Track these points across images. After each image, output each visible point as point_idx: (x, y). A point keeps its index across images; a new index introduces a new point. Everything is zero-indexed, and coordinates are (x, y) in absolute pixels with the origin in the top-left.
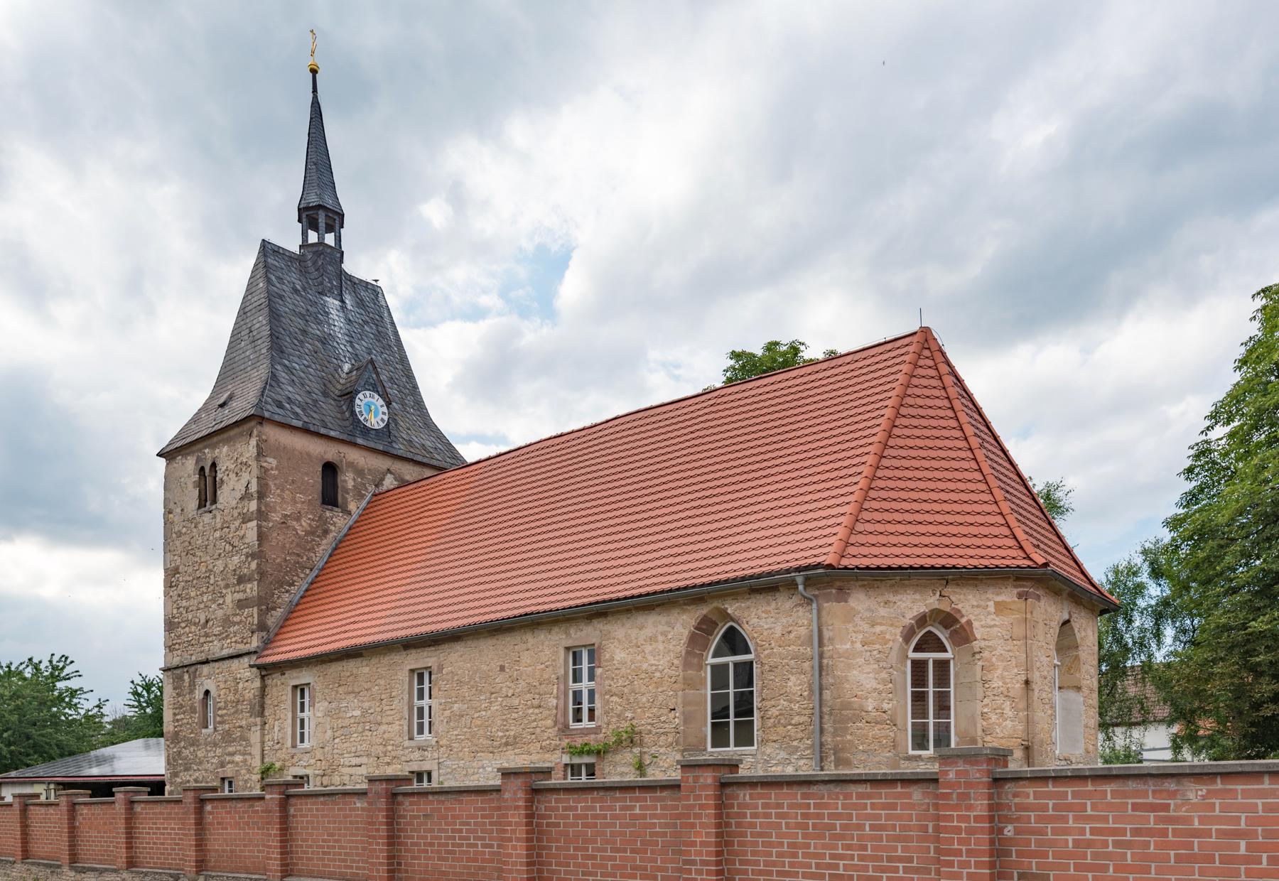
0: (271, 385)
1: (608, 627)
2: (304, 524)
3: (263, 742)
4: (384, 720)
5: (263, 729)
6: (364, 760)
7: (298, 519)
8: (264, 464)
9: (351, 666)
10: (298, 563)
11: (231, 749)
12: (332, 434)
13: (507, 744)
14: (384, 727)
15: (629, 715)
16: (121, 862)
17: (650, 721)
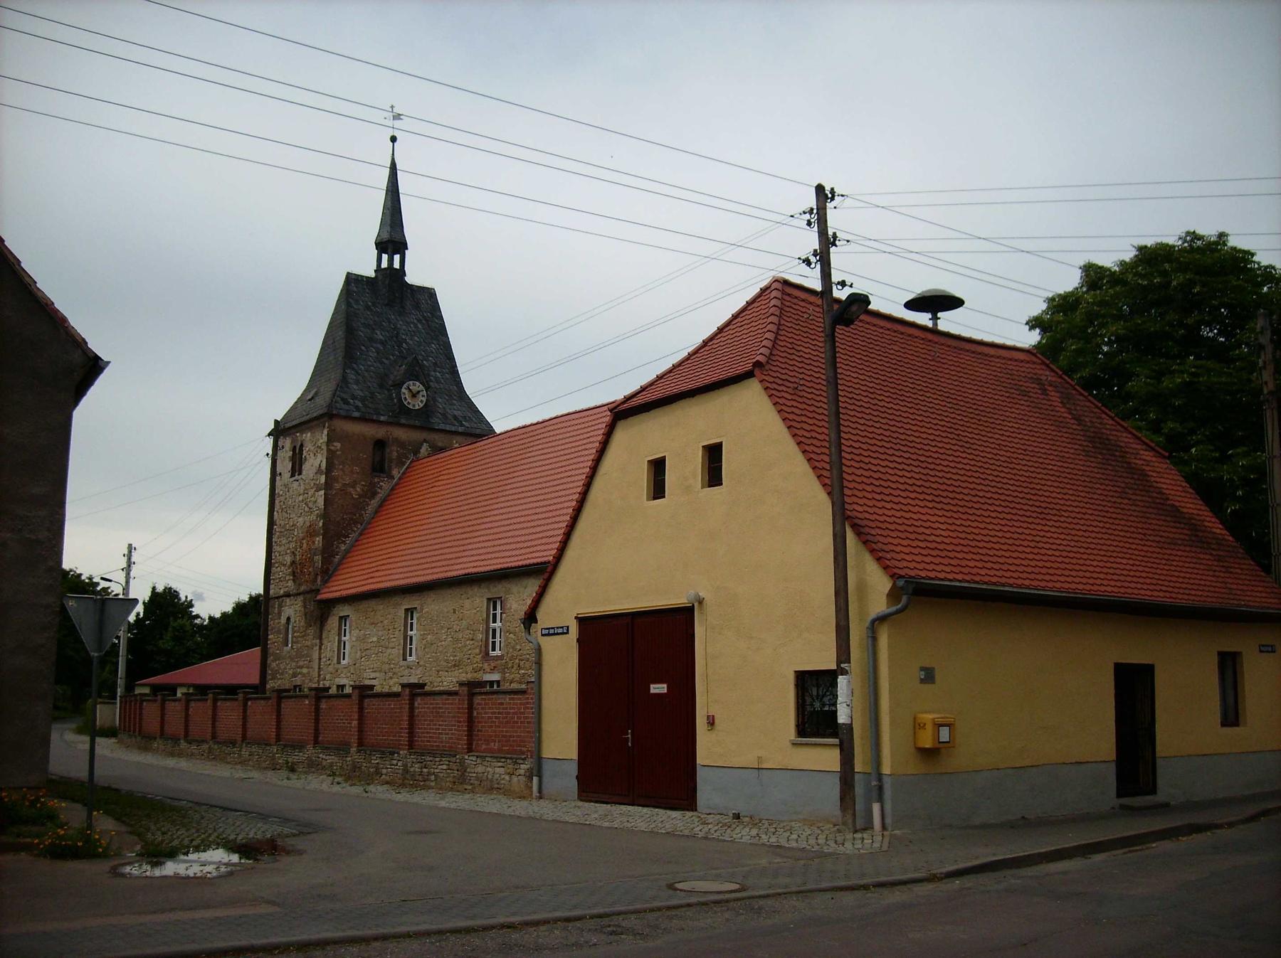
0: (341, 387)
1: (508, 586)
2: (358, 489)
3: (320, 659)
4: (390, 646)
5: (320, 648)
6: (377, 675)
7: (354, 487)
8: (332, 448)
9: (373, 603)
10: (352, 519)
11: (301, 663)
12: (382, 418)
13: (455, 666)
14: (389, 651)
15: (518, 647)
16: (209, 736)
17: (528, 652)
